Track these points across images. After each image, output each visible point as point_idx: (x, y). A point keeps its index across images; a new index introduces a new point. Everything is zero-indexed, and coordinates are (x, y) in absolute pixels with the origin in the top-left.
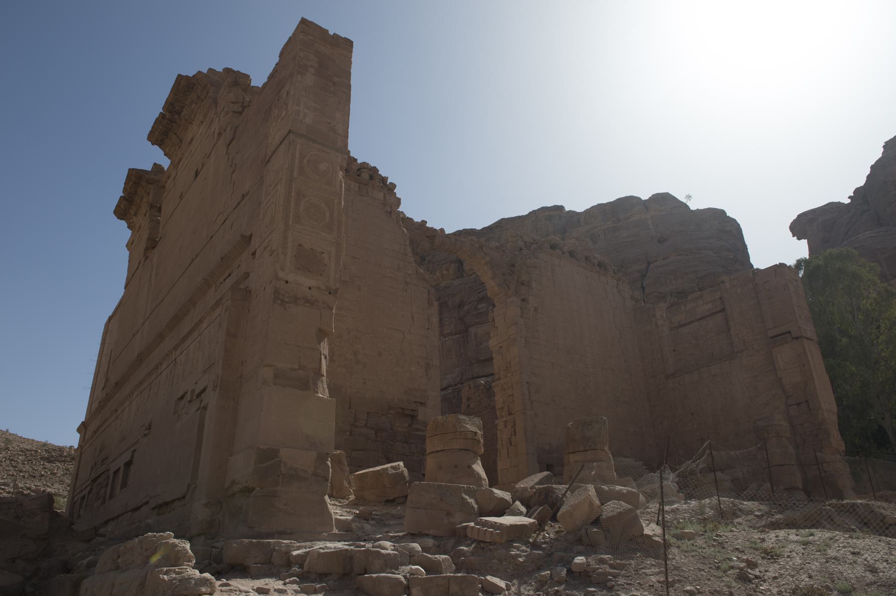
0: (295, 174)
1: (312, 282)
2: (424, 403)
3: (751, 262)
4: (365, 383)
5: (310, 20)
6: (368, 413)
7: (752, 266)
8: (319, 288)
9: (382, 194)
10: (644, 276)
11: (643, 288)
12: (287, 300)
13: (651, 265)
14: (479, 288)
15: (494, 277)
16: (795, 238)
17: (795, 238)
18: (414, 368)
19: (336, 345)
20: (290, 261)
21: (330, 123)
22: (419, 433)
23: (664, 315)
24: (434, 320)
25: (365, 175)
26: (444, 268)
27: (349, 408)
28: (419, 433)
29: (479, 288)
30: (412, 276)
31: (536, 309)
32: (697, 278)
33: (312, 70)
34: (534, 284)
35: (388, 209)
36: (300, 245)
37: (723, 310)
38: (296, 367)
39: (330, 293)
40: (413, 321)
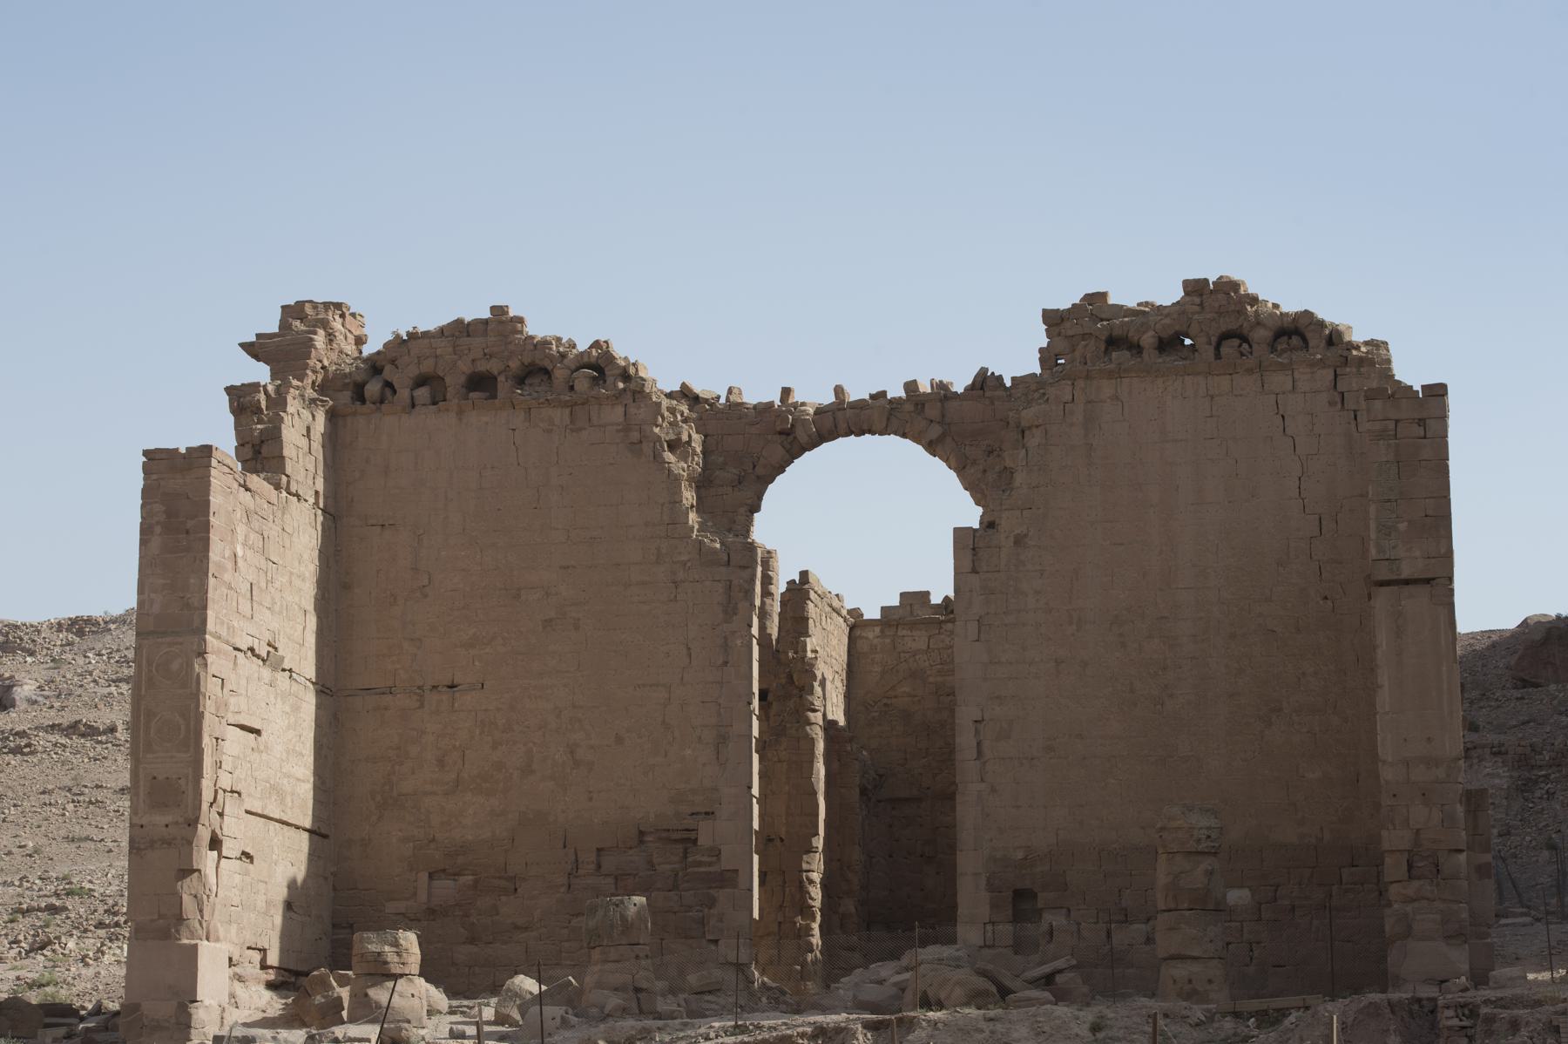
0: (143, 692)
1: (169, 819)
2: (713, 813)
4: (591, 799)
5: (153, 448)
6: (599, 850)
8: (177, 823)
9: (620, 410)
12: (142, 847)
15: (964, 468)
18: (689, 752)
19: (534, 743)
20: (144, 801)
21: (183, 598)
22: (702, 869)
24: (739, 642)
25: (582, 382)
27: (565, 847)
28: (702, 869)
30: (689, 564)
31: (1019, 541)
33: (158, 529)
34: (1019, 478)
35: (635, 436)
36: (155, 778)
38: (156, 917)
39: (189, 825)
40: (690, 655)
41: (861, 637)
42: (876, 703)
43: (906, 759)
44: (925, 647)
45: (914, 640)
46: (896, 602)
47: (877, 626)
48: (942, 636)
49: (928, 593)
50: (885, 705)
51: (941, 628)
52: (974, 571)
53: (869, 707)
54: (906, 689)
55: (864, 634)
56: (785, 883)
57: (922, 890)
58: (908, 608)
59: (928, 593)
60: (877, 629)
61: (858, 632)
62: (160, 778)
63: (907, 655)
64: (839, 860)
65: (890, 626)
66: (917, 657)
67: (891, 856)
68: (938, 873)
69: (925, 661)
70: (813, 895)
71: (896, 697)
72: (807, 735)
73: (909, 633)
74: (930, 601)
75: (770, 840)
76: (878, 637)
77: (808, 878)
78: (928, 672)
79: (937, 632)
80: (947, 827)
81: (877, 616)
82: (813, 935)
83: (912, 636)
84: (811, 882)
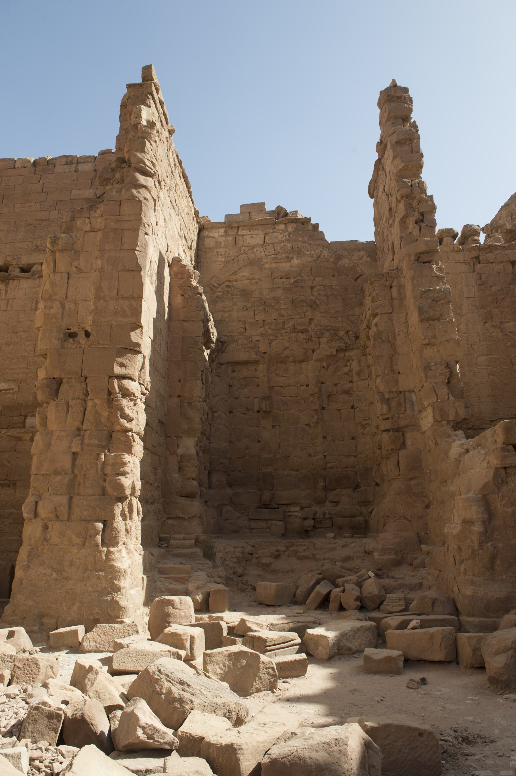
41: (207, 237)
42: (220, 285)
43: (245, 329)
44: (261, 242)
45: (252, 237)
46: (237, 211)
47: (223, 227)
48: (275, 234)
49: (263, 204)
50: (228, 286)
51: (274, 228)
53: (213, 288)
54: (246, 274)
55: (211, 234)
56: (87, 394)
57: (259, 441)
58: (248, 215)
59: (263, 204)
60: (222, 231)
61: (205, 233)
63: (247, 249)
64: (179, 396)
65: (232, 228)
66: (255, 250)
67: (231, 412)
68: (274, 427)
69: (261, 253)
70: (128, 411)
71: (236, 281)
72: (134, 197)
73: (248, 233)
74: (265, 209)
75: (72, 335)
76: (221, 236)
77: (120, 387)
78: (265, 260)
79: (271, 231)
80: (282, 386)
81: (222, 220)
82: (125, 474)
83: (251, 235)
84: (127, 394)
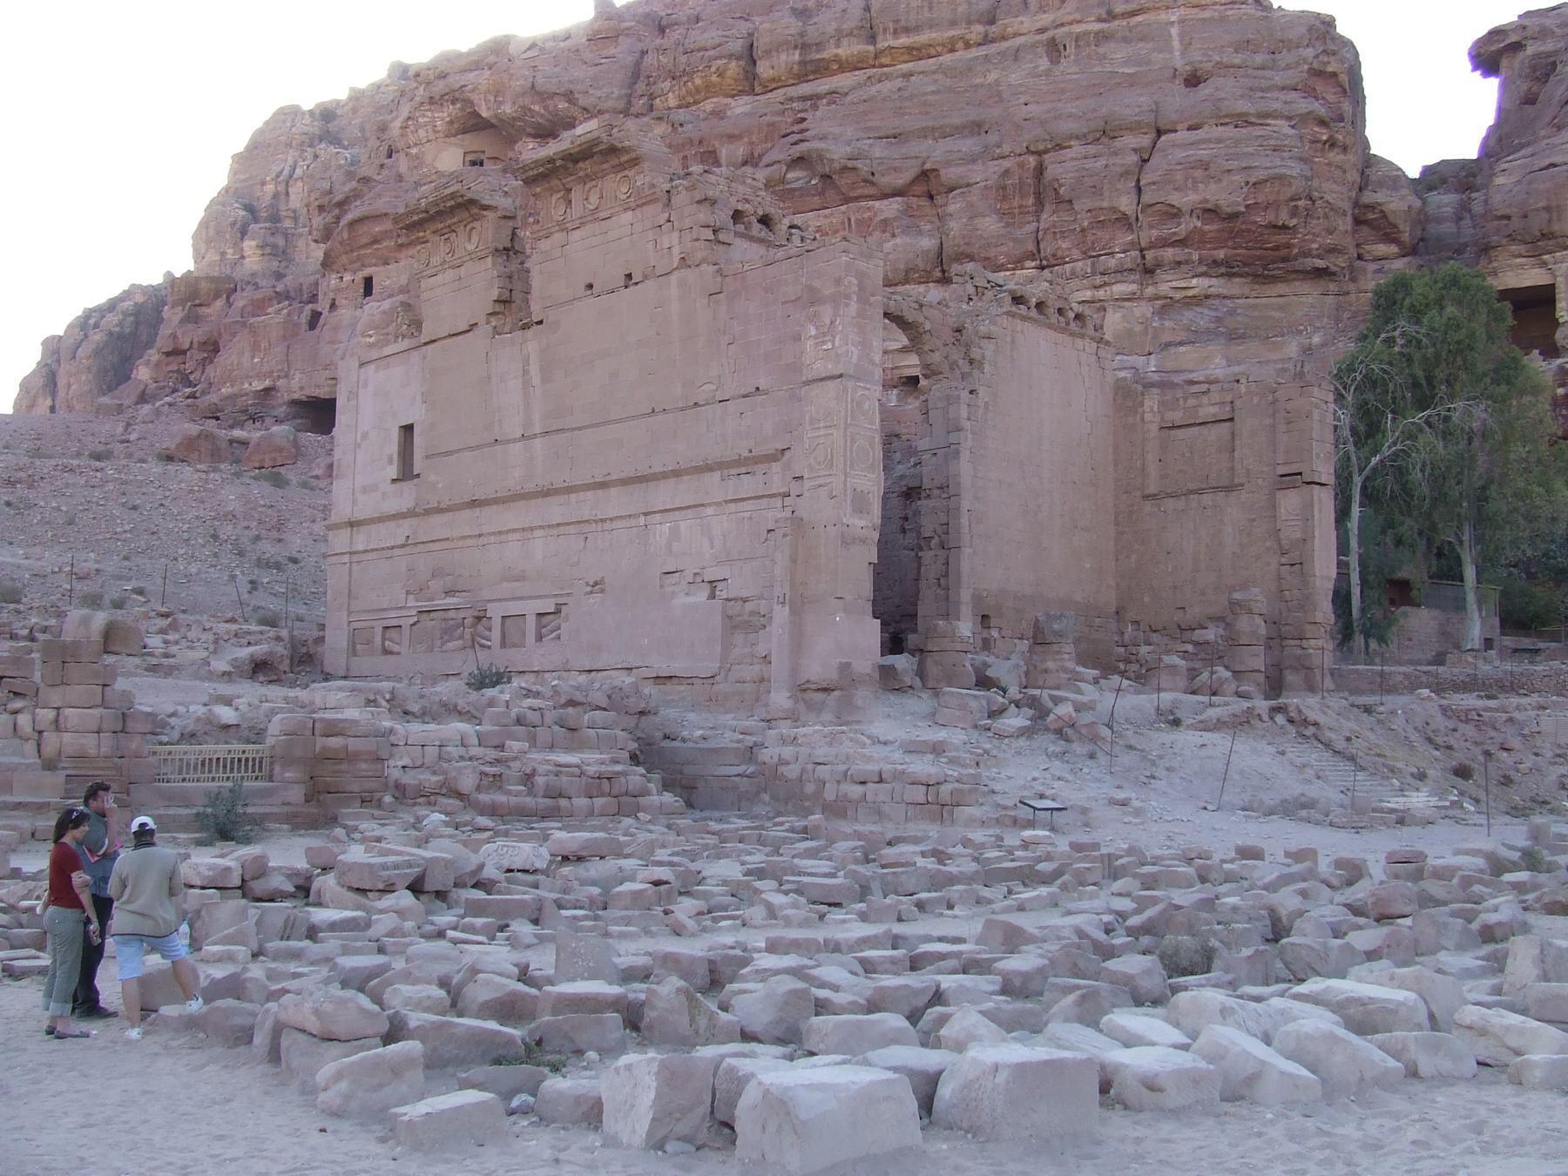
1: (863, 523)
3: (1367, 133)
7: (1367, 146)
10: (1145, 161)
11: (1139, 190)
13: (1163, 138)
14: (793, 133)
16: (1478, 73)
17: (1478, 73)
23: (1155, 409)
26: (713, 69)
29: (793, 133)
31: (986, 404)
32: (1247, 183)
33: (855, 298)
37: (1231, 419)
52: (969, 419)
62: (859, 490)
